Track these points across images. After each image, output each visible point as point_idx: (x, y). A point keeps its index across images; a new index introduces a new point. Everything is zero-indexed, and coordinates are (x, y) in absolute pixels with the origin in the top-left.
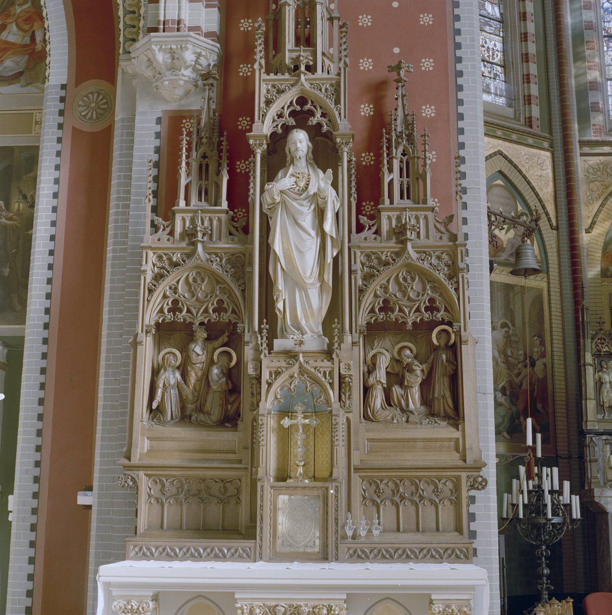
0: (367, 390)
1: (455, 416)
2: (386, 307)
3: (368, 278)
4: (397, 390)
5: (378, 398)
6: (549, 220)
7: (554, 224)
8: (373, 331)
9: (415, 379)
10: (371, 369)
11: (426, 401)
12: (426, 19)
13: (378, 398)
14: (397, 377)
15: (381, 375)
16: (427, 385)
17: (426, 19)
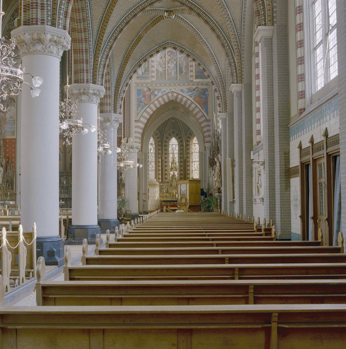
0: (6, 187)
1: (13, 190)
2: (8, 180)
3: (6, 177)
4: (9, 187)
5: (7, 188)
6: (61, 151)
7: (62, 152)
8: (7, 182)
9: (10, 186)
10: (7, 185)
11: (11, 188)
12: (13, 150)
13: (7, 188)
14: (9, 186)
15: (7, 186)
16: (11, 186)
17: (13, 150)
